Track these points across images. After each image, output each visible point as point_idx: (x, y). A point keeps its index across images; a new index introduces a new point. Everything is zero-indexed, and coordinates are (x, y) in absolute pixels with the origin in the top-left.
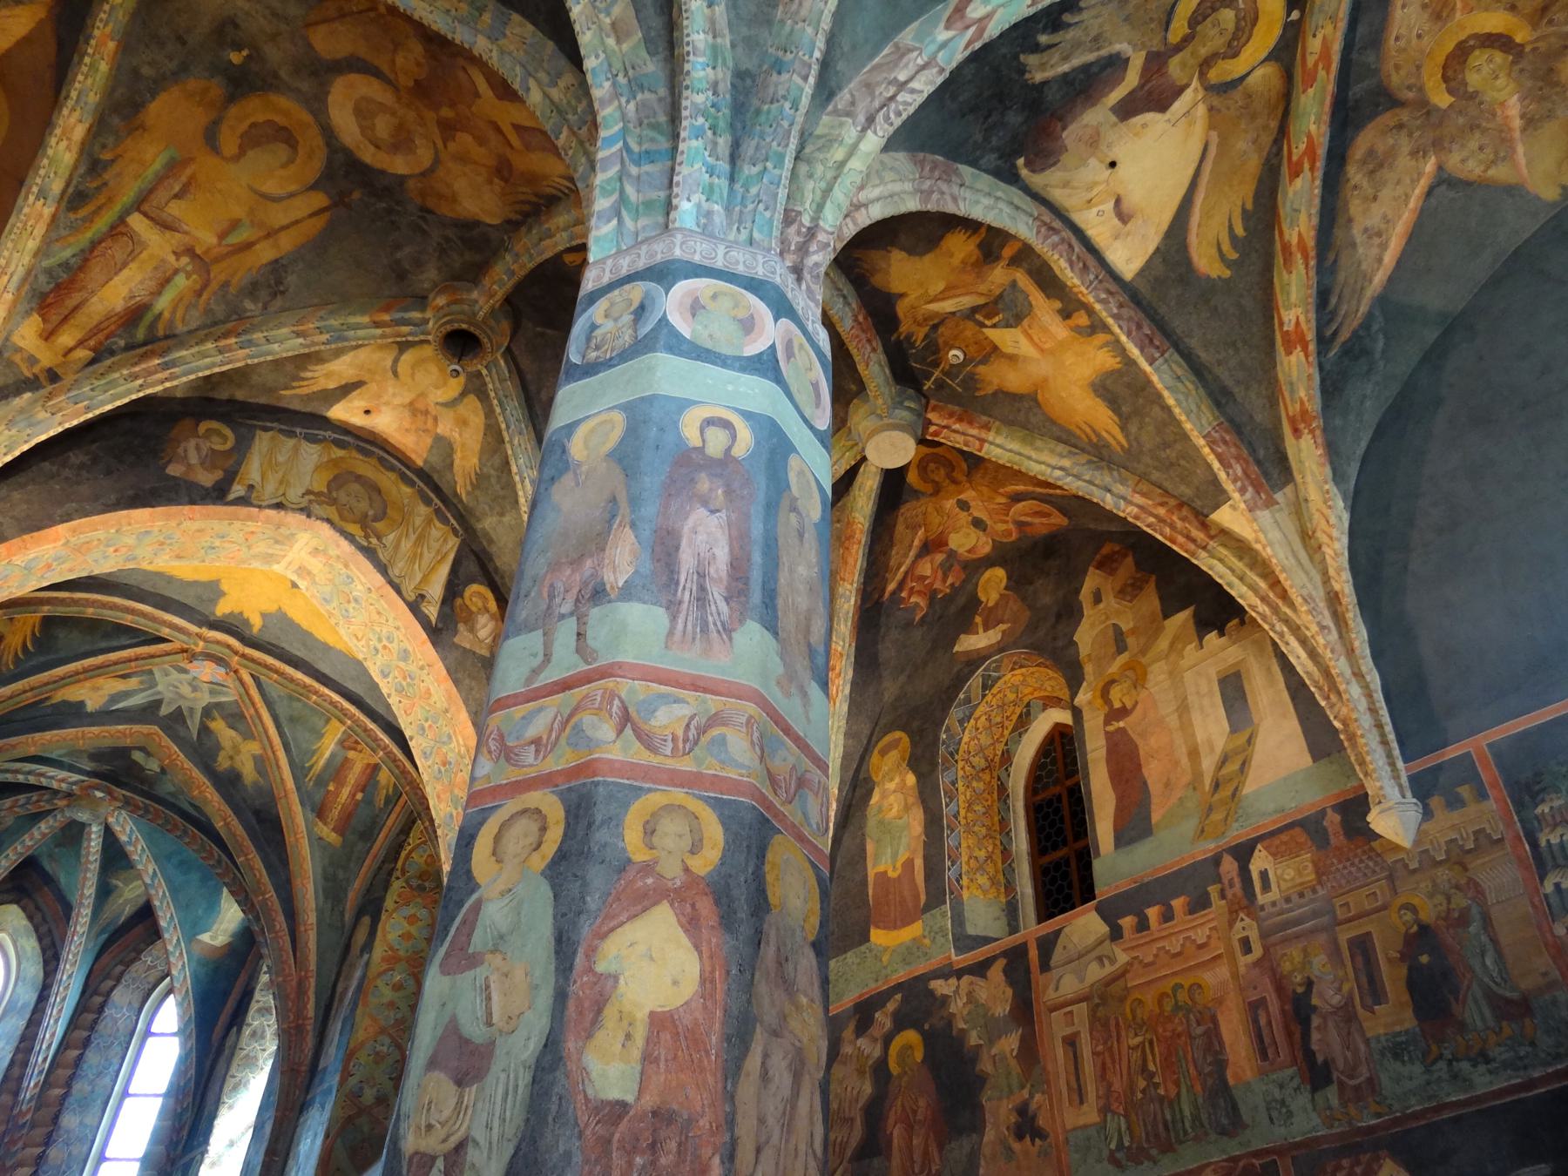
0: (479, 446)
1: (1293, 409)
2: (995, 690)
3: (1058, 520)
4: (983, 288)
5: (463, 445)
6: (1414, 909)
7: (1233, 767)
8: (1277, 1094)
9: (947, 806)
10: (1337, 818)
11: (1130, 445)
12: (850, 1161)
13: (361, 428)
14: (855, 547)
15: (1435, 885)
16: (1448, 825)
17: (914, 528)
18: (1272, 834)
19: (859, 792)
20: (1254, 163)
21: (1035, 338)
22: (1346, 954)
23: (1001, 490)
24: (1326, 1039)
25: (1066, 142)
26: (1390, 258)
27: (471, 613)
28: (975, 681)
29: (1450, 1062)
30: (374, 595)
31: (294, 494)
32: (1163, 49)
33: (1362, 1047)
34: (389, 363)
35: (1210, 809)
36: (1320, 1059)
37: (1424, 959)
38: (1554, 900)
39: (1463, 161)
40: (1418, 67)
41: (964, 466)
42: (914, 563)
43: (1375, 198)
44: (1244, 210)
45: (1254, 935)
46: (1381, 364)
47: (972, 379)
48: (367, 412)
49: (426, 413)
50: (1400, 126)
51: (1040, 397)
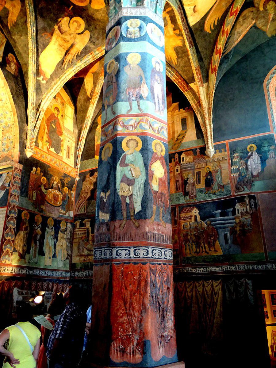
1: (213, 67)
6: (209, 169)
7: (181, 137)
8: (178, 196)
10: (199, 150)
12: (87, 200)
15: (214, 165)
16: (219, 155)
18: (186, 151)
19: (94, 125)
20: (224, 9)
22: (195, 174)
24: (189, 188)
26: (239, 39)
27: (10, 61)
29: (209, 194)
33: (195, 190)
35: (175, 144)
36: (187, 191)
37: (209, 177)
38: (232, 170)
39: (259, 23)
44: (218, 19)
45: (179, 169)
46: (230, 61)
50: (252, 12)
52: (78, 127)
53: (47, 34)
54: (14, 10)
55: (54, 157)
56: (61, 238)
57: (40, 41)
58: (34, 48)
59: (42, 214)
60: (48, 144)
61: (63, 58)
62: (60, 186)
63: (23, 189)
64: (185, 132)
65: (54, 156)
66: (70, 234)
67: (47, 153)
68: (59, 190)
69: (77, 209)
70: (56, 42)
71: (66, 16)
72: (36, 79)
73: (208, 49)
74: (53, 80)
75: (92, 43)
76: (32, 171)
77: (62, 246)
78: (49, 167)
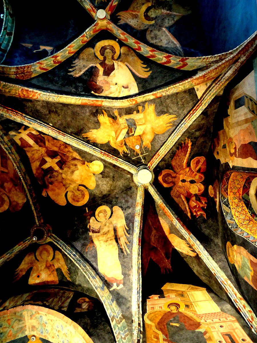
0: (64, 263)
2: (231, 204)
3: (203, 159)
4: (122, 127)
5: (62, 265)
9: (243, 235)
11: (175, 114)
13: (40, 283)
14: (165, 209)
17: (179, 196)
20: (136, 58)
21: (141, 123)
23: (184, 167)
25: (100, 85)
26: (176, 42)
28: (224, 207)
30: (47, 316)
31: (20, 302)
32: (101, 62)
34: (34, 258)
40: (143, 24)
41: (171, 171)
42: (188, 205)
43: (161, 40)
44: (143, 64)
47: (146, 148)
48: (38, 276)
49: (51, 265)
50: (151, 31)
51: (157, 133)
52: (225, 300)
53: (88, 246)
54: (61, 263)
57: (89, 257)
58: (85, 267)
61: (118, 247)
64: (247, 97)
70: (100, 243)
71: (90, 219)
72: (110, 291)
73: (166, 74)
74: (129, 275)
75: (127, 210)
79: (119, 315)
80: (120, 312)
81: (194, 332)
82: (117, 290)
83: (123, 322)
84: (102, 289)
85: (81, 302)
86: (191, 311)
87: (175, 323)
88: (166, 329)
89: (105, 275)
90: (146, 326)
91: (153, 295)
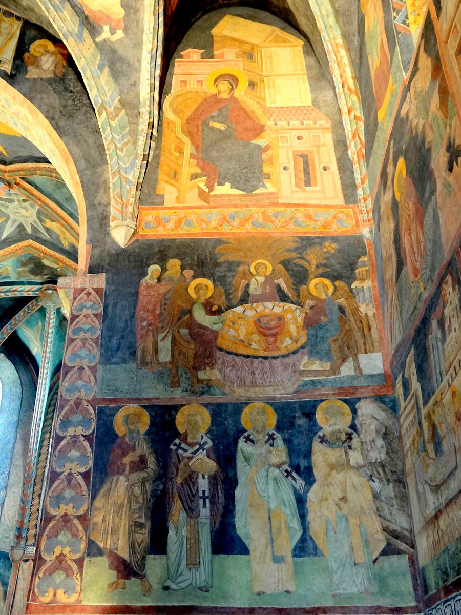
27: (36, 57)
55: (235, 206)
56: (332, 467)
59: (207, 398)
60: (202, 183)
62: (284, 286)
63: (115, 342)
65: (239, 203)
66: (380, 442)
67: (199, 208)
68: (284, 298)
69: (390, 341)
72: (96, 44)
74: (137, 11)
76: (147, 278)
77: (344, 499)
78: (219, 242)
79: (113, 101)
80: (115, 93)
81: (247, 144)
82: (112, 42)
83: (121, 117)
84: (80, 37)
85: (39, 52)
86: (256, 97)
87: (219, 122)
88: (200, 133)
89: (83, 2)
90: (165, 124)
91: (190, 50)
